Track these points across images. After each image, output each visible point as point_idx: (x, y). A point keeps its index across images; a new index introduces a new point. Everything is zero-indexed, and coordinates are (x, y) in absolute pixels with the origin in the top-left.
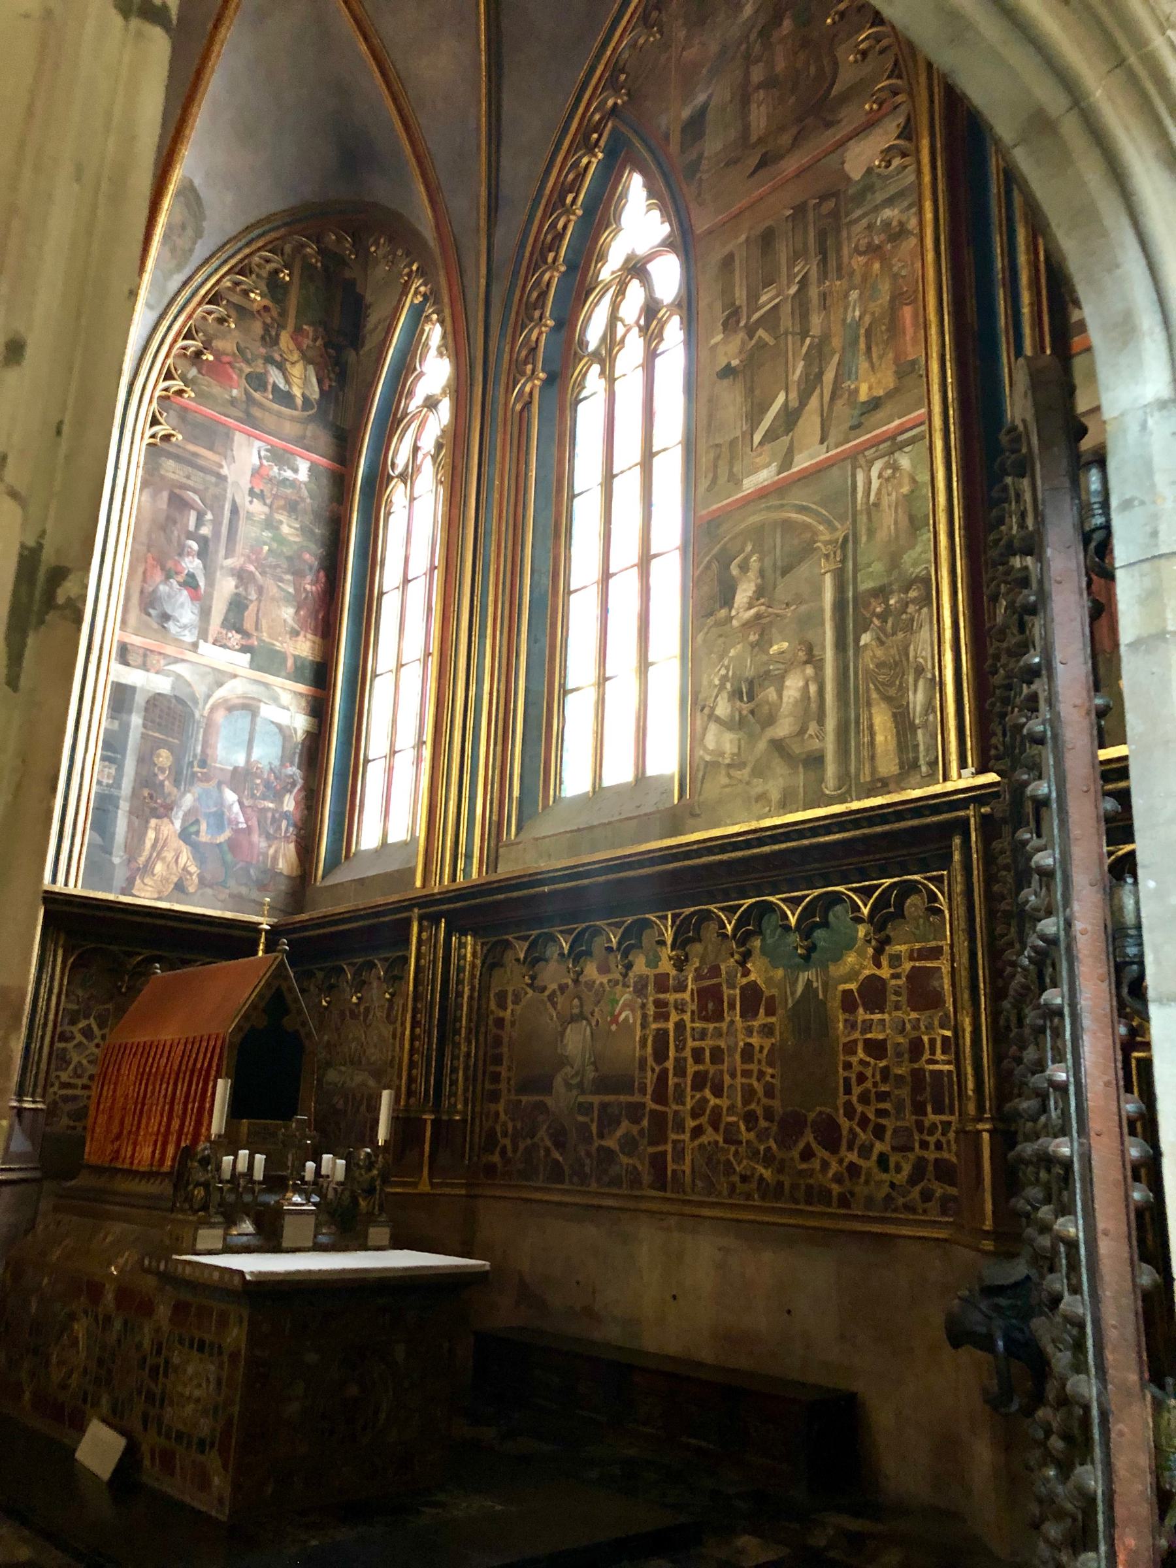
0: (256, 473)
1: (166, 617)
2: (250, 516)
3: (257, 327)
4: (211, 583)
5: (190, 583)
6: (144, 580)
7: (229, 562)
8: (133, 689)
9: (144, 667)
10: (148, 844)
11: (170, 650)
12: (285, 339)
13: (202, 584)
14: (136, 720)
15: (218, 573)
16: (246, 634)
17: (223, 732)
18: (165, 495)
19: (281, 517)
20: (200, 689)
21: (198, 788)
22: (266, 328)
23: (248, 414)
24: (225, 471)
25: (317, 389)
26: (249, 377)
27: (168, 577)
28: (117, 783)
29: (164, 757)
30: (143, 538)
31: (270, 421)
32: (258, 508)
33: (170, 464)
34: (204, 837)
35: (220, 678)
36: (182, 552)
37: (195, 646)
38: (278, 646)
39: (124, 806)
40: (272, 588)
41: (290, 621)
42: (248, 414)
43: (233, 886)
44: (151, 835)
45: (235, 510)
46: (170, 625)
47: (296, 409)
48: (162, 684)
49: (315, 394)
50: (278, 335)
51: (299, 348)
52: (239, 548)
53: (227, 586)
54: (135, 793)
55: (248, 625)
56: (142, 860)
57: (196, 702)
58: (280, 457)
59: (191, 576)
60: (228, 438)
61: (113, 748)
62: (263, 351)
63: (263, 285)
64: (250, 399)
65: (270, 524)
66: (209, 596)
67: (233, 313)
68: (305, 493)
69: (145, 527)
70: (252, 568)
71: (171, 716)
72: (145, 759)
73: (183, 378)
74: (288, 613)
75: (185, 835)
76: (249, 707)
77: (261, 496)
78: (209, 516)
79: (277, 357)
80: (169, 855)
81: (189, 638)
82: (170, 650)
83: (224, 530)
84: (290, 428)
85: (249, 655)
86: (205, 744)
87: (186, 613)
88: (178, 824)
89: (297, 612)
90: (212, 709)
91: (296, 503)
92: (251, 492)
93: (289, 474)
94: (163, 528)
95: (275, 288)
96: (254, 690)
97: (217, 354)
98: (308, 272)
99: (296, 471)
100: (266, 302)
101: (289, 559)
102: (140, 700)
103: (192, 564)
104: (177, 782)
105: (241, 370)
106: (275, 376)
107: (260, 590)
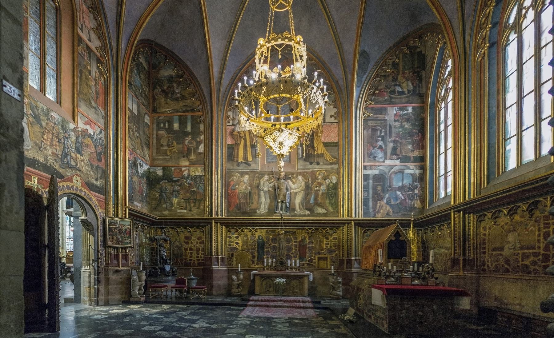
0: (395, 115)
1: (375, 157)
2: (395, 126)
3: (391, 78)
4: (386, 146)
5: (380, 147)
6: (368, 150)
7: (390, 140)
8: (369, 175)
9: (371, 169)
10: (378, 207)
11: (377, 164)
12: (400, 78)
13: (383, 147)
14: (371, 181)
15: (388, 143)
16: (398, 155)
17: (395, 179)
18: (370, 130)
19: (405, 123)
20: (387, 171)
21: (389, 193)
22: (393, 77)
23: (391, 102)
24: (386, 118)
25: (412, 86)
26: (390, 92)
27: (374, 148)
28: (368, 195)
29: (379, 188)
30: (366, 141)
31: (398, 101)
32: (397, 124)
33: (371, 123)
34: (393, 202)
35: (392, 167)
36: (377, 141)
37: (384, 162)
38: (408, 155)
39: (371, 200)
40: (404, 142)
41: (411, 148)
42: (391, 102)
43: (402, 212)
44: (379, 205)
45: (390, 127)
46: (377, 159)
47: (405, 94)
48: (376, 172)
49: (411, 88)
50: (397, 78)
51: (404, 77)
52: (393, 135)
53: (391, 145)
54: (373, 197)
55: (398, 152)
56: (377, 210)
57: (386, 174)
58: (401, 109)
59: (380, 146)
60: (386, 109)
61: (366, 188)
62: (393, 84)
63: (390, 66)
64: (391, 98)
65: (401, 126)
66: (386, 149)
67: (383, 78)
68: (411, 115)
69: (366, 139)
70: (397, 139)
71: (380, 179)
72: (374, 189)
73: (371, 100)
74: (410, 147)
75: (387, 203)
76: (401, 172)
77: (398, 121)
78: (383, 130)
79: (398, 83)
80: (384, 208)
81: (382, 160)
82: (377, 164)
83: (388, 132)
84: (403, 100)
85: (399, 160)
86: (390, 183)
87: (380, 155)
88: (385, 201)
89: (413, 145)
90: (391, 174)
91: (409, 119)
92: (395, 121)
93: (406, 112)
94: (371, 137)
95: (395, 65)
96: (402, 167)
97: (380, 91)
98: (405, 56)
99: (408, 110)
100: (392, 71)
101: (409, 133)
102: (371, 177)
103: (381, 143)
104: (383, 192)
105: (387, 91)
106: (398, 89)
107: (401, 143)
